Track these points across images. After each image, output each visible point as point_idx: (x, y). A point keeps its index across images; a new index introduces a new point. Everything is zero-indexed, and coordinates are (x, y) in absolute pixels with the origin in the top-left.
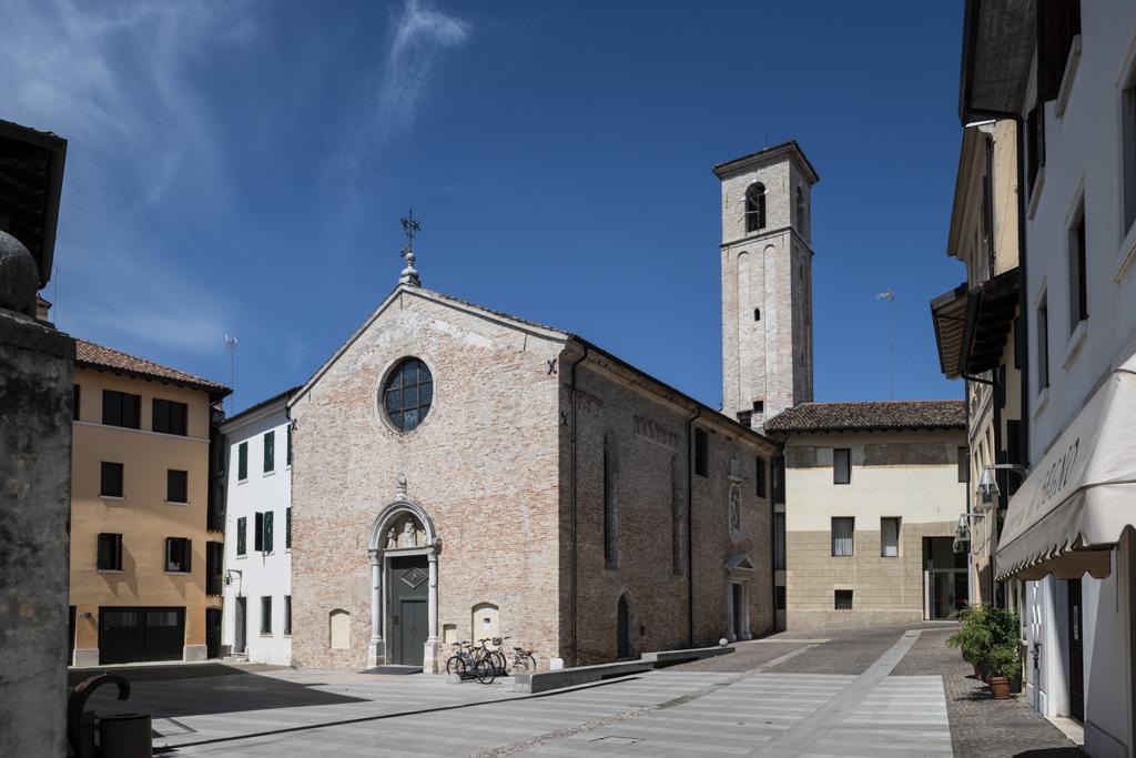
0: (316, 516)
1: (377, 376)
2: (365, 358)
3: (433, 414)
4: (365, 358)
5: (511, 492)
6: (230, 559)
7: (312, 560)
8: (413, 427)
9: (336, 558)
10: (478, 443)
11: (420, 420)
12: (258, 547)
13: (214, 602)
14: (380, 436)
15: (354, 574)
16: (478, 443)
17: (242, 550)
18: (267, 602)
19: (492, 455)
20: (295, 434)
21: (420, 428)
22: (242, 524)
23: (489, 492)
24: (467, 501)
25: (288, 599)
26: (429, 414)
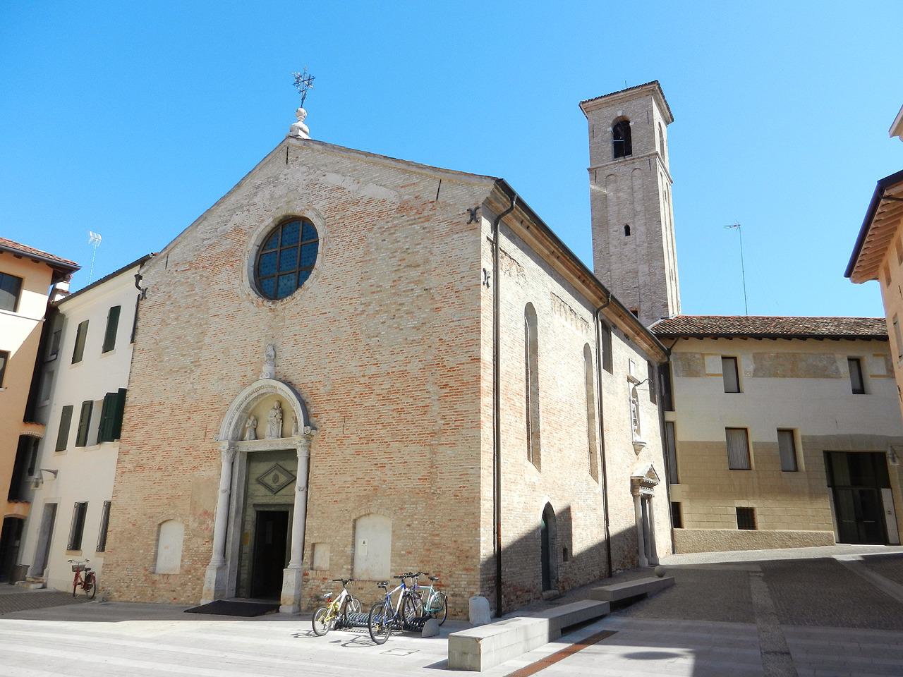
0: (156, 401)
1: (250, 237)
2: (237, 219)
3: (317, 276)
4: (237, 219)
5: (415, 367)
6: (48, 457)
8: (290, 292)
10: (371, 310)
11: (299, 285)
13: (17, 509)
14: (246, 304)
16: (371, 310)
17: (61, 446)
18: (82, 509)
19: (390, 322)
20: (144, 304)
21: (298, 294)
22: (67, 411)
23: (384, 368)
24: (353, 379)
25: (108, 506)
26: (312, 276)
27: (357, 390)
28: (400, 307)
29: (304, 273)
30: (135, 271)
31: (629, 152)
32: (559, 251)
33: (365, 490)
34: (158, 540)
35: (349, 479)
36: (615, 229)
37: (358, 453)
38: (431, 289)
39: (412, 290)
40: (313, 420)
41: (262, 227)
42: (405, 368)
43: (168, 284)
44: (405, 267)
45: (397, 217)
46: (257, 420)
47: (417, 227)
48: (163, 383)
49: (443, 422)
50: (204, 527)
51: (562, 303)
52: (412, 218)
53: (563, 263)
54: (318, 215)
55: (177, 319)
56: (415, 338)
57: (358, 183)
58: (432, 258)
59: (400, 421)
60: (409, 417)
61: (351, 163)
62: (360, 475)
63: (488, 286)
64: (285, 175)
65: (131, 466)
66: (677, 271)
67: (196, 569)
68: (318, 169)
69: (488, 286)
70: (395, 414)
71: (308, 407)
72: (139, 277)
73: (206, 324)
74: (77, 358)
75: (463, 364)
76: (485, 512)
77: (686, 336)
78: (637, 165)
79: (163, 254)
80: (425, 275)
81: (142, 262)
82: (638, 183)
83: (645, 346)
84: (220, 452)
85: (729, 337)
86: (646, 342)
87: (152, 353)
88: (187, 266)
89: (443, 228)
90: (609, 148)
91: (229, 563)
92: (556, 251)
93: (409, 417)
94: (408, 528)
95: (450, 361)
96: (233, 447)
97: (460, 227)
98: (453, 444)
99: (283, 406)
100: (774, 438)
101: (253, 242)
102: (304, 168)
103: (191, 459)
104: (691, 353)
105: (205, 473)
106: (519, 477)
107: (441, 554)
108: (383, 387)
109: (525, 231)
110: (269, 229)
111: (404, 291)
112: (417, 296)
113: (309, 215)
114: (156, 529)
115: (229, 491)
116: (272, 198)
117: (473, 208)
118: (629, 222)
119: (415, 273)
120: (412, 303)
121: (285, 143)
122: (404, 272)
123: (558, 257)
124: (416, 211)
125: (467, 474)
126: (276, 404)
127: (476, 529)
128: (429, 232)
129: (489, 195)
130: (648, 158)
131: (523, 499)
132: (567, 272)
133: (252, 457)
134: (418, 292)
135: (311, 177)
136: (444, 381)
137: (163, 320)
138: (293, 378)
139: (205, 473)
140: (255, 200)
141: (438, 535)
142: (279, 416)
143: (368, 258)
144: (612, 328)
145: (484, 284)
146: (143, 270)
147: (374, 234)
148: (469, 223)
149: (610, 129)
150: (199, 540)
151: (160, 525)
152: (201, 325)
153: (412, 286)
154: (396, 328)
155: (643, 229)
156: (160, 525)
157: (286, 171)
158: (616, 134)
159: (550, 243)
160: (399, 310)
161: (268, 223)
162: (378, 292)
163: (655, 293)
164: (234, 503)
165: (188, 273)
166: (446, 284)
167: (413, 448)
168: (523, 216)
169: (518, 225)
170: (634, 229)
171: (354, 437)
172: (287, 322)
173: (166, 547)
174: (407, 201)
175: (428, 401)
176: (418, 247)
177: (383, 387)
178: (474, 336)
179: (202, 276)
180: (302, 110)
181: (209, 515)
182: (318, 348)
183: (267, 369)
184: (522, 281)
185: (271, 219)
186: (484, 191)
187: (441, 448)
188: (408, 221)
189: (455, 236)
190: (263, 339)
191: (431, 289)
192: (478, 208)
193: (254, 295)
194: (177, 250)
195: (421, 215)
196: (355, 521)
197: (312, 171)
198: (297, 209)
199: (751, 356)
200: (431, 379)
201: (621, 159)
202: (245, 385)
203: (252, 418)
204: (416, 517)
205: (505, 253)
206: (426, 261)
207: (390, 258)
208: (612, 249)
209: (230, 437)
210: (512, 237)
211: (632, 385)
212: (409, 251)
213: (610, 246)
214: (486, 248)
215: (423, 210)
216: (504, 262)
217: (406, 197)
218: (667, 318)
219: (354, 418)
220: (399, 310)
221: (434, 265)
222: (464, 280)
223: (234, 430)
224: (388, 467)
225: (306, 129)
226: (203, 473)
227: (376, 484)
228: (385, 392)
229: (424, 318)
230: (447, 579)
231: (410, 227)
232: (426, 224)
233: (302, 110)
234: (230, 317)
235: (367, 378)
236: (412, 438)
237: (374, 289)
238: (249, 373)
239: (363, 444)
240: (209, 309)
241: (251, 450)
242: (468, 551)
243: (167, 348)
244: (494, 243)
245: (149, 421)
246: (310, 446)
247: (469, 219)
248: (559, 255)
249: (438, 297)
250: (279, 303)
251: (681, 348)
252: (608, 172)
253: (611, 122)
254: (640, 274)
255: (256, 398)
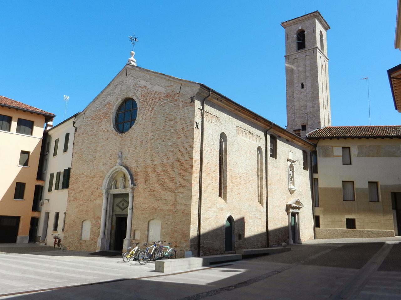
1: (113, 106)
2: (109, 99)
3: (137, 124)
4: (109, 99)
5: (170, 161)
7: (77, 194)
8: (127, 130)
9: (87, 194)
11: (131, 127)
12: (55, 189)
15: (95, 202)
21: (130, 131)
23: (160, 162)
27: (150, 170)
28: (166, 137)
29: (133, 121)
30: (73, 120)
31: (304, 47)
32: (240, 108)
33: (152, 210)
34: (82, 227)
35: (147, 205)
36: (297, 85)
37: (150, 195)
38: (177, 130)
39: (170, 130)
40: (135, 182)
41: (118, 102)
42: (167, 162)
43: (85, 126)
44: (168, 120)
45: (165, 100)
46: (116, 181)
47: (172, 104)
48: (83, 166)
49: (179, 184)
50: (97, 223)
51: (244, 130)
52: (171, 100)
53: (243, 113)
54: (137, 98)
55: (88, 140)
56: (171, 150)
57: (152, 85)
58: (178, 117)
59: (164, 183)
60: (168, 181)
61: (149, 76)
62: (150, 204)
63: (198, 129)
64: (126, 81)
65: (72, 199)
66: (329, 104)
67: (95, 239)
68: (138, 79)
69: (198, 129)
70: (163, 180)
71: (133, 177)
72: (74, 123)
73: (98, 142)
74: (55, 154)
75: (187, 161)
76: (194, 219)
77: (324, 138)
78: (308, 53)
79: (82, 113)
80: (175, 124)
81: (75, 116)
82: (308, 62)
83: (300, 144)
84: (103, 194)
85: (345, 138)
86: (300, 142)
87: (79, 154)
88: (91, 118)
89: (181, 104)
90: (295, 45)
91: (106, 236)
92: (238, 108)
93: (168, 181)
94: (166, 225)
95: (183, 159)
96: (107, 192)
97: (188, 104)
98: (183, 193)
99: (126, 176)
100: (366, 186)
101: (114, 109)
102: (133, 78)
103: (93, 196)
104: (327, 146)
105: (98, 202)
106: (213, 205)
107: (177, 235)
108: (159, 169)
109: (220, 103)
110: (120, 103)
111: (167, 131)
112: (172, 133)
113: (134, 98)
114: (81, 223)
115: (106, 209)
116: (121, 90)
117: (192, 96)
118: (303, 81)
119: (171, 123)
120: (170, 135)
121: (126, 67)
122: (168, 122)
123: (240, 111)
124: (172, 97)
125: (187, 204)
126: (122, 175)
127: (189, 225)
128: (177, 106)
129: (198, 91)
130: (313, 50)
131: (215, 214)
132: (246, 116)
133: (115, 196)
134: (172, 131)
135: (135, 82)
136: (180, 167)
137: (83, 141)
138: (129, 165)
139: (98, 202)
140: (115, 91)
141: (176, 227)
142: (123, 180)
143: (155, 117)
144: (278, 138)
145: (196, 128)
146: (75, 120)
147: (157, 106)
148: (191, 103)
149: (295, 36)
150: (96, 228)
151: (83, 222)
152: (96, 143)
153: (170, 128)
154: (164, 145)
155: (310, 85)
156: (83, 222)
157: (126, 79)
158: (298, 39)
159: (234, 105)
160: (165, 138)
161: (120, 101)
162: (158, 131)
163: (314, 116)
164: (108, 213)
165: (92, 121)
166: (182, 128)
167: (169, 193)
168: (218, 97)
169: (216, 101)
170: (306, 85)
171: (149, 189)
172: (126, 142)
173: (85, 230)
174: (169, 93)
175: (175, 175)
176: (173, 112)
177: (159, 169)
178: (191, 149)
179: (96, 122)
180: (133, 52)
181: (99, 218)
182: (137, 153)
183: (119, 161)
184: (218, 124)
185: (121, 99)
186: (197, 89)
187: (179, 194)
188: (169, 101)
189: (186, 108)
190: (118, 149)
191: (177, 130)
192: (194, 97)
193: (114, 131)
194: (88, 111)
195: (174, 99)
196: (149, 222)
197: (135, 79)
198: (130, 96)
199: (357, 147)
200: (176, 166)
201: (300, 51)
202: (111, 167)
203: (114, 180)
204: (169, 220)
205: (209, 113)
206: (175, 118)
207: (163, 117)
208: (295, 95)
209: (106, 188)
210: (213, 106)
211: (290, 163)
212: (169, 114)
213: (294, 94)
214: (198, 113)
215: (175, 97)
216: (207, 118)
217: (169, 91)
218: (319, 128)
219: (149, 181)
220: (165, 138)
221: (178, 120)
222: (188, 126)
223: (108, 185)
224: (160, 201)
225: (134, 60)
226: (97, 202)
227: (156, 207)
228: (160, 171)
229: (174, 142)
230: (179, 244)
231: (170, 104)
232: (176, 103)
233: (133, 52)
234: (107, 140)
235: (154, 165)
236: (169, 190)
237: (157, 129)
238: (113, 163)
239: (151, 192)
240: (99, 136)
241: (114, 193)
242: (186, 234)
243: (85, 152)
244: (202, 110)
245: (79, 181)
246: (134, 192)
247: (191, 101)
248: (241, 110)
249: (179, 133)
250: (123, 134)
251: (321, 144)
252: (294, 57)
253: (296, 32)
254: (308, 107)
255: (115, 173)
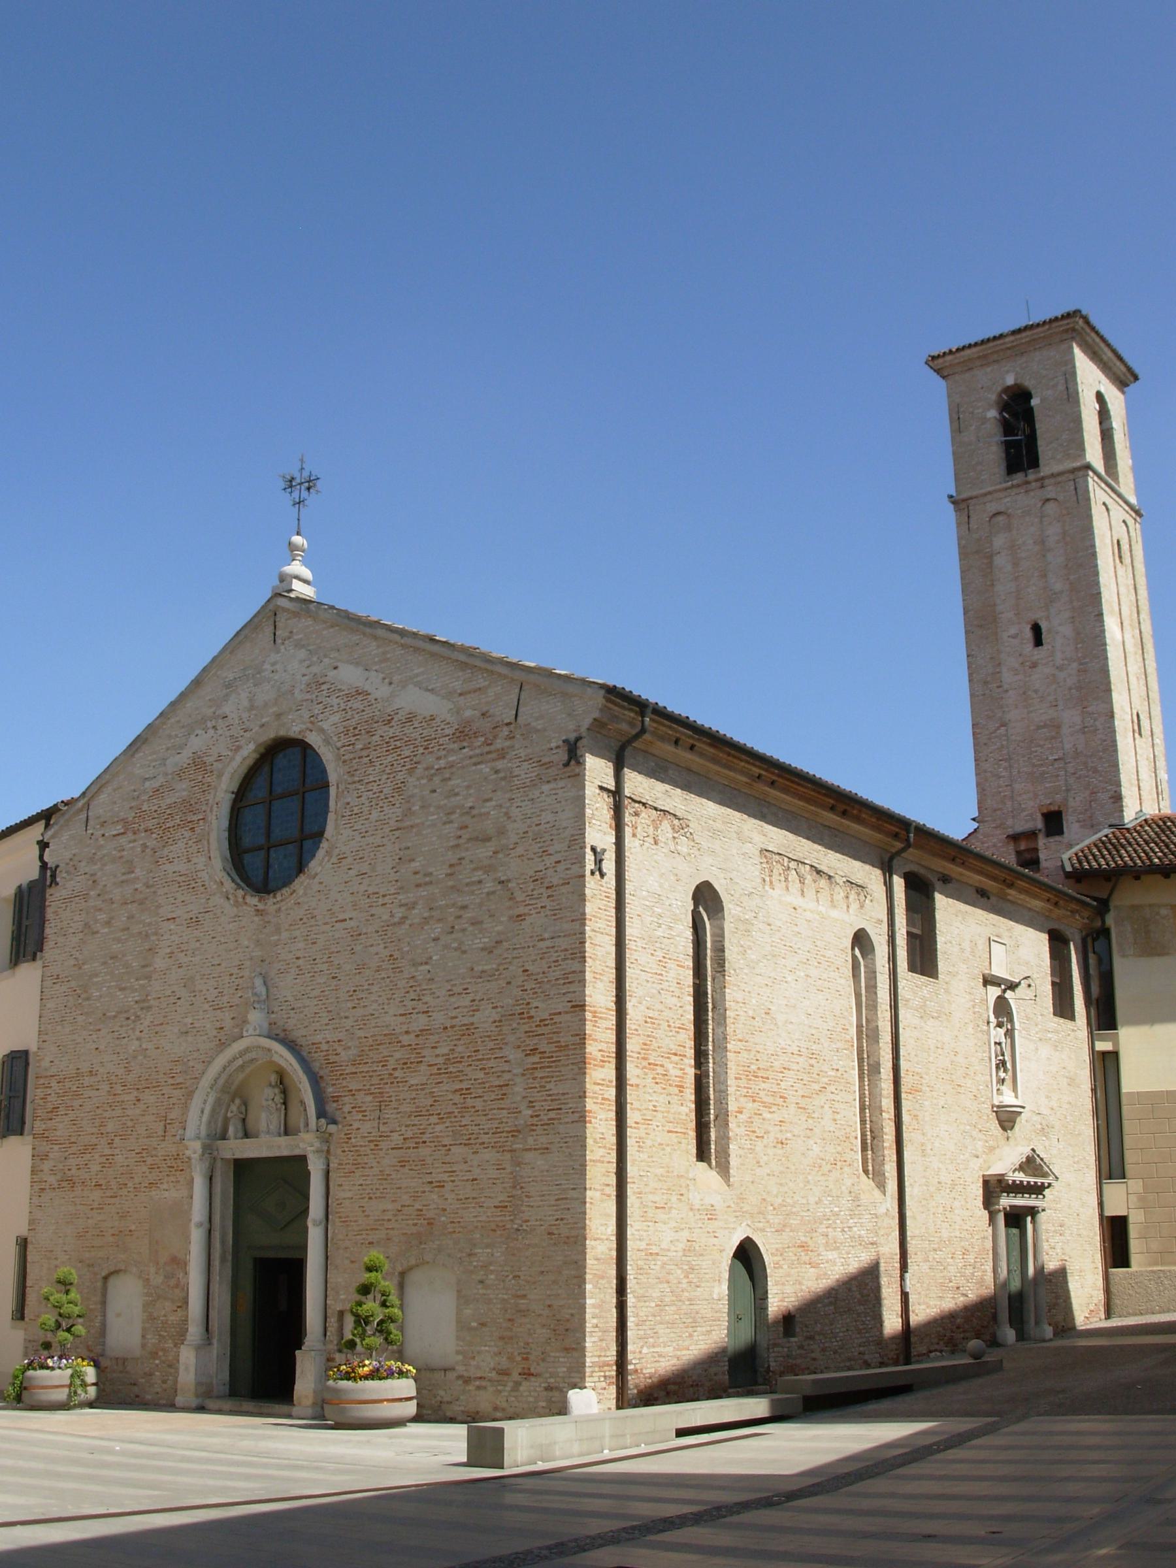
1: (220, 776)
2: (197, 743)
3: (328, 853)
5: (486, 1017)
11: (300, 868)
14: (218, 900)
21: (301, 884)
23: (439, 1019)
26: (320, 853)
27: (398, 1055)
28: (462, 912)
29: (308, 844)
32: (773, 773)
33: (415, 1225)
34: (104, 1303)
35: (390, 1206)
36: (1013, 631)
37: (403, 1163)
38: (509, 881)
39: (480, 882)
40: (331, 1107)
41: (238, 759)
42: (471, 1020)
43: (92, 860)
45: (452, 750)
46: (245, 1103)
47: (485, 769)
48: (94, 1037)
49: (530, 1112)
50: (173, 1282)
51: (793, 865)
52: (478, 751)
53: (785, 790)
54: (327, 742)
55: (108, 923)
56: (486, 968)
57: (390, 683)
60: (479, 1104)
61: (378, 647)
63: (602, 875)
64: (273, 664)
65: (52, 1180)
66: (1157, 710)
68: (325, 656)
69: (602, 875)
70: (457, 1098)
71: (323, 1085)
72: (43, 845)
73: (156, 934)
75: (560, 1013)
76: (597, 1259)
77: (1135, 874)
79: (80, 804)
80: (500, 856)
81: (47, 816)
83: (1037, 904)
84: (189, 1158)
86: (1035, 897)
87: (73, 984)
88: (119, 828)
90: (993, 454)
91: (215, 1341)
92: (763, 772)
93: (479, 1104)
94: (480, 1286)
95: (542, 1009)
96: (208, 1149)
97: (553, 771)
99: (286, 1081)
101: (224, 786)
102: (302, 654)
103: (145, 1169)
104: (1150, 905)
105: (169, 1193)
106: (674, 1199)
107: (529, 1326)
108: (438, 1051)
109: (688, 756)
110: (250, 762)
111: (467, 885)
112: (488, 894)
113: (313, 739)
114: (99, 1284)
115: (207, 1225)
116: (252, 707)
117: (572, 736)
118: (1038, 615)
119: (483, 852)
120: (481, 905)
121: (271, 607)
122: (467, 850)
123: (773, 783)
124: (483, 739)
125: (566, 1199)
126: (273, 1078)
127: (580, 1287)
128: (504, 778)
129: (596, 715)
131: (685, 1234)
132: (801, 803)
133: (242, 1167)
134: (489, 886)
135: (315, 669)
136: (531, 1042)
137: (87, 925)
138: (298, 1034)
139: (169, 1193)
140: (227, 709)
141: (524, 1296)
142: (279, 1099)
143: (409, 823)
144: (938, 885)
145: (593, 873)
146: (50, 833)
147: (418, 779)
148: (567, 765)
150: (167, 1304)
151: (106, 1278)
152: (147, 935)
153: (479, 875)
154: (456, 949)
155: (1067, 630)
156: (106, 1278)
157: (274, 657)
159: (748, 763)
160: (460, 917)
161: (248, 752)
162: (426, 884)
163: (1095, 771)
164: (217, 1244)
165: (123, 840)
166: (531, 873)
167: (488, 1155)
168: (677, 731)
169: (670, 748)
170: (1049, 631)
171: (395, 1136)
172: (285, 935)
173: (118, 1315)
174: (469, 722)
175: (507, 1076)
176: (488, 804)
177: (438, 1051)
178: (576, 966)
179: (145, 846)
180: (298, 540)
181: (179, 1263)
182: (335, 982)
183: (256, 1017)
184: (684, 846)
185: (252, 746)
186: (590, 709)
187: (529, 1156)
188: (471, 757)
189: (546, 788)
190: (248, 963)
191: (509, 881)
192: (578, 739)
193: (229, 885)
194: (103, 797)
195: (492, 748)
196: (403, 1274)
197: (315, 659)
198: (294, 730)
200: (511, 1038)
202: (222, 1045)
203: (237, 1101)
204: (492, 1268)
205: (644, 804)
206: (501, 832)
207: (445, 823)
208: (1007, 677)
209: (203, 1133)
210: (658, 771)
211: (994, 992)
212: (474, 812)
213: (1004, 670)
214: (598, 809)
215: (495, 737)
217: (468, 713)
218: (1120, 827)
219: (394, 1104)
220: (460, 917)
221: (513, 838)
222: (560, 867)
223: (209, 1123)
224: (449, 1186)
225: (307, 573)
226: (166, 1194)
227: (430, 1214)
228: (440, 1060)
229: (499, 933)
230: (538, 1364)
231: (474, 768)
232: (500, 764)
233: (298, 540)
234: (194, 922)
235: (412, 1036)
236: (485, 1138)
237: (419, 878)
238: (228, 1024)
239: (409, 1148)
240: (159, 906)
241: (238, 1156)
242: (568, 1320)
243: (96, 975)
244: (617, 795)
245: (76, 1103)
246: (328, 1151)
247: (566, 757)
248: (774, 778)
249: (520, 896)
250: (271, 900)
251: (1127, 897)
252: (992, 507)
254: (1065, 730)
255: (242, 1067)
